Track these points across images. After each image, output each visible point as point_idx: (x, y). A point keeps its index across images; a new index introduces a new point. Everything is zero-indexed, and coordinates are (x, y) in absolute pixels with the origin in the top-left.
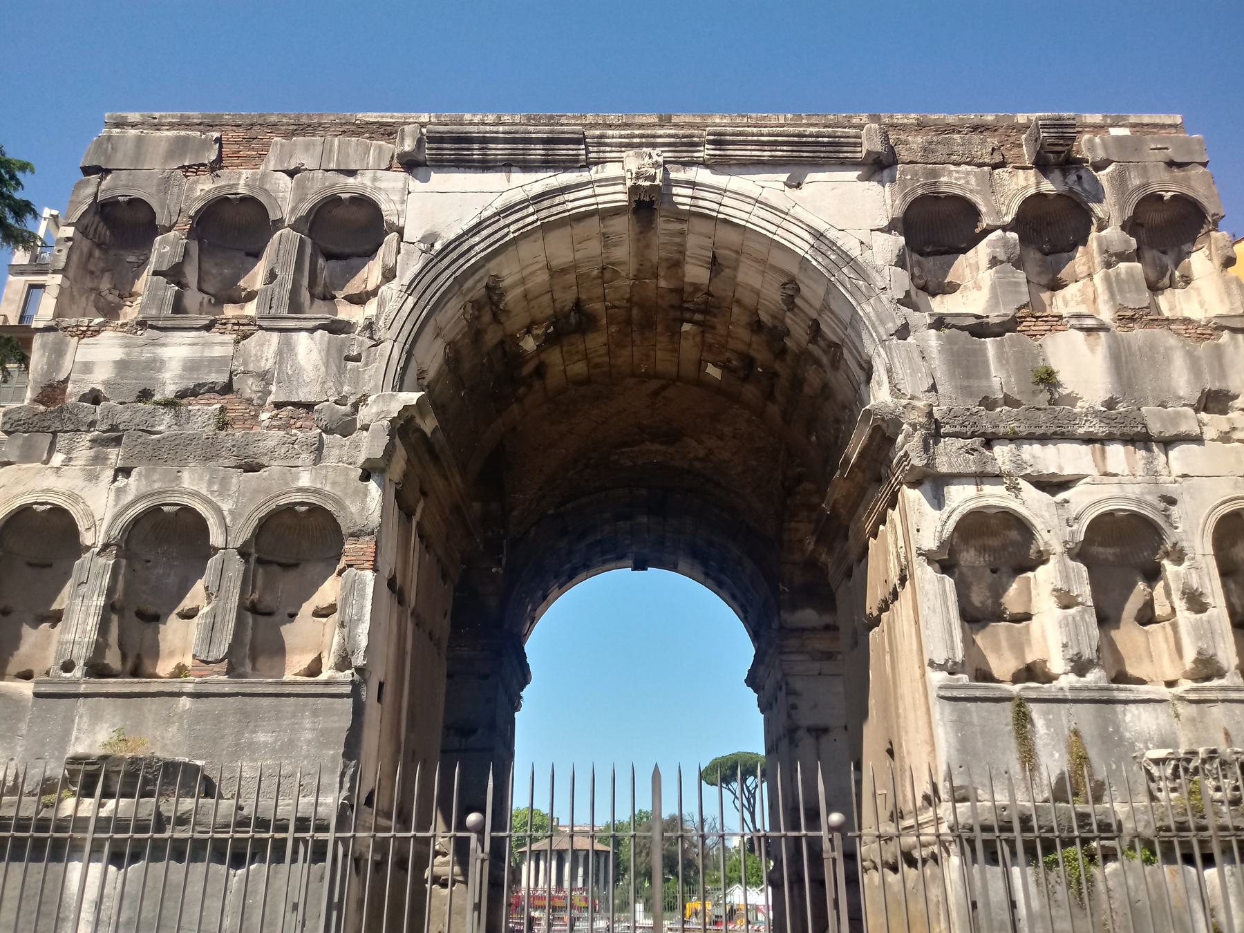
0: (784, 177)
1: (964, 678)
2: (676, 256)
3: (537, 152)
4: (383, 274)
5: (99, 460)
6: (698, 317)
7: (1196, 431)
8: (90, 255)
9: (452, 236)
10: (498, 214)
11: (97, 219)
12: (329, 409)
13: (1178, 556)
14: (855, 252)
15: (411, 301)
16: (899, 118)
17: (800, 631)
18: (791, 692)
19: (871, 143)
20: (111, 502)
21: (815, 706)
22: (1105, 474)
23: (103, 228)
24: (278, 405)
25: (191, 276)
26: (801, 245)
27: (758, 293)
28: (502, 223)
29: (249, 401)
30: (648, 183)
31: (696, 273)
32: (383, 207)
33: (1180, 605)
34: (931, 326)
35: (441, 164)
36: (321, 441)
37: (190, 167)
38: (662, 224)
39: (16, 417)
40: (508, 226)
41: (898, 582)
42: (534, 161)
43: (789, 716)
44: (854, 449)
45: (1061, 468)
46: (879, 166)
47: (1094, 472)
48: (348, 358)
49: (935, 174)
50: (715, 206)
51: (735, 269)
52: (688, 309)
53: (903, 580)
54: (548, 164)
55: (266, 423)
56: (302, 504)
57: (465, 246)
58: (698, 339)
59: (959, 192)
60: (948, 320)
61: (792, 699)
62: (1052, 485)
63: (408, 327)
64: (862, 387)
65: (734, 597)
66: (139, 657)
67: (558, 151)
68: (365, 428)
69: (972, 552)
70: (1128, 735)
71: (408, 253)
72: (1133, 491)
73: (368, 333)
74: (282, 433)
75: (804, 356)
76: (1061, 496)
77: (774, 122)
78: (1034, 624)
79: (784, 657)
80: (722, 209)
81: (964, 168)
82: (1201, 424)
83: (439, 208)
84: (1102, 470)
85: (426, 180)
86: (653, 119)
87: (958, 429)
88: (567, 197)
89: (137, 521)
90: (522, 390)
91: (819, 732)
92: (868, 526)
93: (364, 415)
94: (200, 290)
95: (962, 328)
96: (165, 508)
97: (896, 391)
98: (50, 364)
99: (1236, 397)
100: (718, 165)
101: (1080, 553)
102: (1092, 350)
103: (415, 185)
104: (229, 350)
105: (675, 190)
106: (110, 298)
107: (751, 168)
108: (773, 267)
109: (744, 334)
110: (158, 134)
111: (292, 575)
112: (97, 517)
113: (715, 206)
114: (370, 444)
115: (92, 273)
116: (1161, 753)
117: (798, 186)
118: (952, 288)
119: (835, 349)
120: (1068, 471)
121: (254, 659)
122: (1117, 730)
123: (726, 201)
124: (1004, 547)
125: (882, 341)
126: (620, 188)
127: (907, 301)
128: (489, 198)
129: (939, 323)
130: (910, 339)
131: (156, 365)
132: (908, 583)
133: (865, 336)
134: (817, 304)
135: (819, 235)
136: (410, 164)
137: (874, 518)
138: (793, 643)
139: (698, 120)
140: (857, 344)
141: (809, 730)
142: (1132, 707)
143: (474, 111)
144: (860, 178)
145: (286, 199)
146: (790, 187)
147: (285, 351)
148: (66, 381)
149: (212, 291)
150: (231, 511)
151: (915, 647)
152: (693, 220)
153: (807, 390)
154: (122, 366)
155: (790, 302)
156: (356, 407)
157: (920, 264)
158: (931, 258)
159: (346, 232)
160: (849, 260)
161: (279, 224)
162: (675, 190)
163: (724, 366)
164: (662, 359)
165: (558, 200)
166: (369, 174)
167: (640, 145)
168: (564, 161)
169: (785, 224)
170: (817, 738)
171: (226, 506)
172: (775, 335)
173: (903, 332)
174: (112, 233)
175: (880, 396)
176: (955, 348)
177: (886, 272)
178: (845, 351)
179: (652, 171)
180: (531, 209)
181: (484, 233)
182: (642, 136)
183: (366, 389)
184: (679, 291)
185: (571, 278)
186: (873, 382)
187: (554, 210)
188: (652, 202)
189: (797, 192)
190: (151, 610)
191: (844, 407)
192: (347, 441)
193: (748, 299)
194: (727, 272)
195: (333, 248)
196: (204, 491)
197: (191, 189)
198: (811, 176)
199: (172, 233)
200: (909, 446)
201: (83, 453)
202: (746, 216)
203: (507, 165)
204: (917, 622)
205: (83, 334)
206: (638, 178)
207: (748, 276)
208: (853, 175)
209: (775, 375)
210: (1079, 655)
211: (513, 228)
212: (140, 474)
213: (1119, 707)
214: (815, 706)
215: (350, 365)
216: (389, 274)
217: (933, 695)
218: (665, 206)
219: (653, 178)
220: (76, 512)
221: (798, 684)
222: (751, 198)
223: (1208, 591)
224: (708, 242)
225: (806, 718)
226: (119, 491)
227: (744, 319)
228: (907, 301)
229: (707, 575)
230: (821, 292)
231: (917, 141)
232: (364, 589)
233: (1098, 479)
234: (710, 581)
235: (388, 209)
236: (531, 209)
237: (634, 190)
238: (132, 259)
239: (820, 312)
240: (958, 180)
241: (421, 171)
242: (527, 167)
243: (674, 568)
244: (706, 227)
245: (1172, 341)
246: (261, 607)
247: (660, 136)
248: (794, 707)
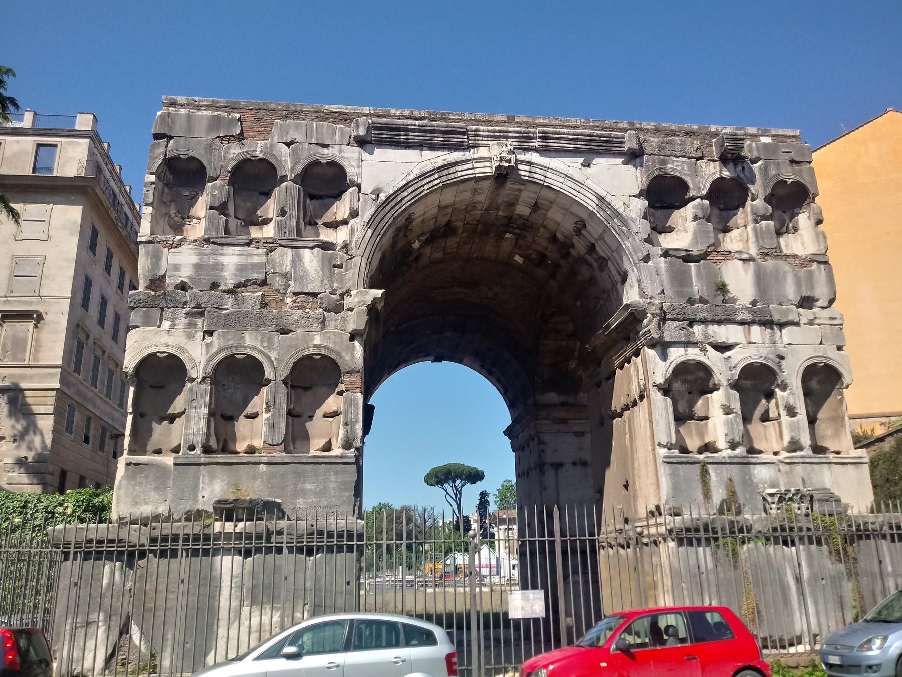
0: (581, 160)
1: (676, 452)
2: (513, 200)
3: (439, 139)
4: (350, 213)
5: (192, 325)
6: (517, 231)
7: (796, 320)
8: (163, 192)
9: (392, 192)
10: (417, 178)
11: (166, 168)
13: (784, 387)
14: (621, 210)
15: (370, 232)
16: (645, 125)
17: (548, 406)
18: (541, 442)
19: (630, 144)
20: (204, 352)
21: (555, 451)
23: (168, 173)
24: (296, 294)
25: (231, 210)
27: (559, 224)
28: (420, 184)
29: (278, 291)
30: (507, 165)
31: (522, 209)
32: (347, 170)
33: (783, 413)
34: (662, 256)
35: (382, 143)
37: (224, 137)
38: (509, 184)
39: (137, 298)
40: (423, 185)
41: (637, 398)
42: (437, 144)
43: (540, 457)
44: (615, 322)
45: (727, 339)
46: (634, 157)
47: (744, 341)
48: (335, 266)
49: (664, 163)
50: (543, 178)
51: (547, 210)
52: (512, 227)
53: (642, 397)
54: (445, 147)
55: (290, 305)
56: (317, 354)
57: (399, 198)
58: (513, 242)
59: (678, 174)
60: (671, 252)
61: (541, 447)
62: (722, 347)
63: (369, 248)
64: (619, 285)
65: (499, 381)
66: (225, 441)
67: (451, 139)
68: (351, 310)
69: (679, 382)
70: (755, 481)
71: (365, 200)
72: (764, 351)
73: (345, 250)
75: (581, 260)
76: (727, 354)
77: (574, 124)
78: (710, 422)
79: (538, 422)
80: (546, 179)
81: (681, 159)
82: (799, 315)
83: (383, 171)
85: (372, 153)
86: (504, 118)
87: (675, 316)
88: (460, 168)
89: (220, 363)
90: (405, 268)
91: (558, 466)
92: (617, 363)
93: (348, 302)
94: (235, 217)
95: (678, 257)
97: (643, 294)
98: (152, 264)
99: (818, 300)
100: (543, 151)
101: (735, 385)
102: (746, 272)
103: (365, 156)
104: (263, 259)
105: (520, 167)
106: (176, 219)
107: (562, 154)
108: (572, 213)
109: (544, 243)
110: (200, 113)
111: (309, 394)
112: (197, 361)
113: (543, 178)
115: (165, 203)
116: (773, 491)
117: (589, 166)
118: (671, 230)
119: (603, 262)
120: (731, 341)
121: (294, 442)
122: (750, 479)
123: (549, 174)
124: (695, 380)
125: (636, 264)
126: (488, 164)
127: (649, 240)
128: (411, 167)
129: (666, 253)
130: (650, 263)
132: (645, 399)
133: (625, 258)
134: (596, 236)
135: (601, 199)
136: (362, 143)
137: (622, 359)
138: (544, 413)
139: (530, 120)
140: (619, 262)
141: (552, 465)
142: (758, 466)
143: (397, 108)
144: (623, 163)
145: (287, 162)
146: (584, 166)
147: (297, 261)
148: (164, 276)
149: (241, 217)
150: (275, 358)
151: (649, 433)
152: (528, 184)
153: (579, 277)
154: (198, 267)
155: (578, 232)
156: (342, 296)
157: (653, 214)
158: (659, 211)
160: (618, 215)
161: (284, 178)
162: (520, 167)
163: (527, 258)
164: (489, 250)
165: (452, 170)
166: (337, 147)
167: (499, 137)
168: (455, 145)
169: (582, 190)
170: (556, 470)
171: (273, 355)
172: (565, 248)
173: (647, 259)
174: (174, 177)
175: (631, 296)
176: (675, 269)
178: (610, 263)
179: (509, 157)
180: (437, 176)
181: (410, 190)
182: (500, 132)
183: (348, 286)
184: (510, 218)
185: (450, 210)
186: (626, 284)
187: (450, 177)
188: (507, 174)
189: (588, 170)
190: (229, 413)
191: (604, 292)
193: (551, 226)
194: (542, 211)
195: (313, 192)
196: (259, 346)
197: (227, 153)
198: (597, 161)
199: (218, 182)
200: (650, 325)
201: (182, 321)
202: (560, 185)
203: (420, 146)
204: (651, 421)
206: (501, 161)
207: (555, 214)
208: (620, 161)
209: (557, 266)
211: (426, 187)
212: (219, 335)
213: (752, 466)
214: (555, 451)
215: (337, 270)
216: (354, 214)
217: (660, 461)
218: (514, 176)
219: (509, 161)
220: (184, 357)
221: (546, 438)
222: (562, 172)
223: (798, 406)
224: (535, 196)
225: (550, 457)
226: (209, 346)
227: (546, 235)
228: (649, 240)
229: (482, 366)
230: (600, 231)
231: (655, 141)
232: (357, 404)
234: (484, 371)
235: (351, 171)
236: (437, 176)
237: (499, 168)
238: (186, 193)
239: (597, 240)
240: (677, 167)
241: (368, 147)
242: (433, 148)
243: (460, 361)
244: (536, 188)
245: (787, 268)
246: (294, 412)
247: (511, 132)
248: (543, 451)
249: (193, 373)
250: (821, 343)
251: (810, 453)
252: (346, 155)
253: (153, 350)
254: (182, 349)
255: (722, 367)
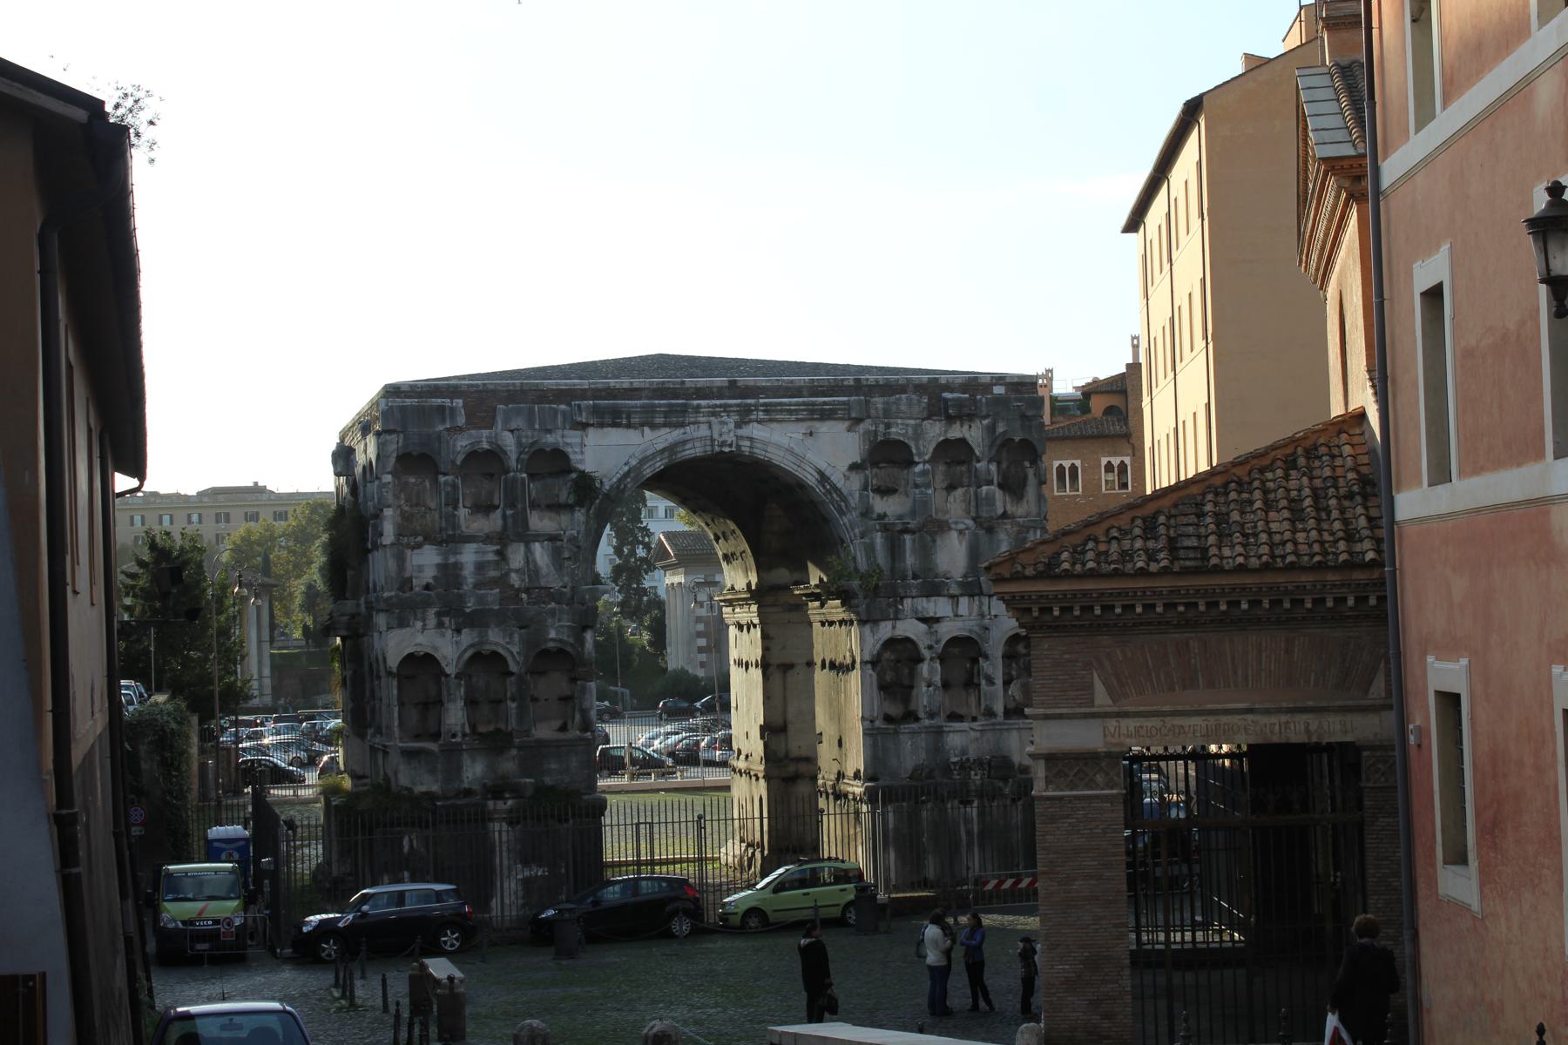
5: (440, 625)
13: (986, 657)
26: (811, 479)
33: (983, 682)
101: (942, 658)
131: (458, 566)
135: (821, 473)
166: (560, 432)
177: (857, 495)
201: (432, 621)
205: (413, 548)
240: (899, 430)
249: (448, 670)
252: (568, 440)
254: (436, 649)
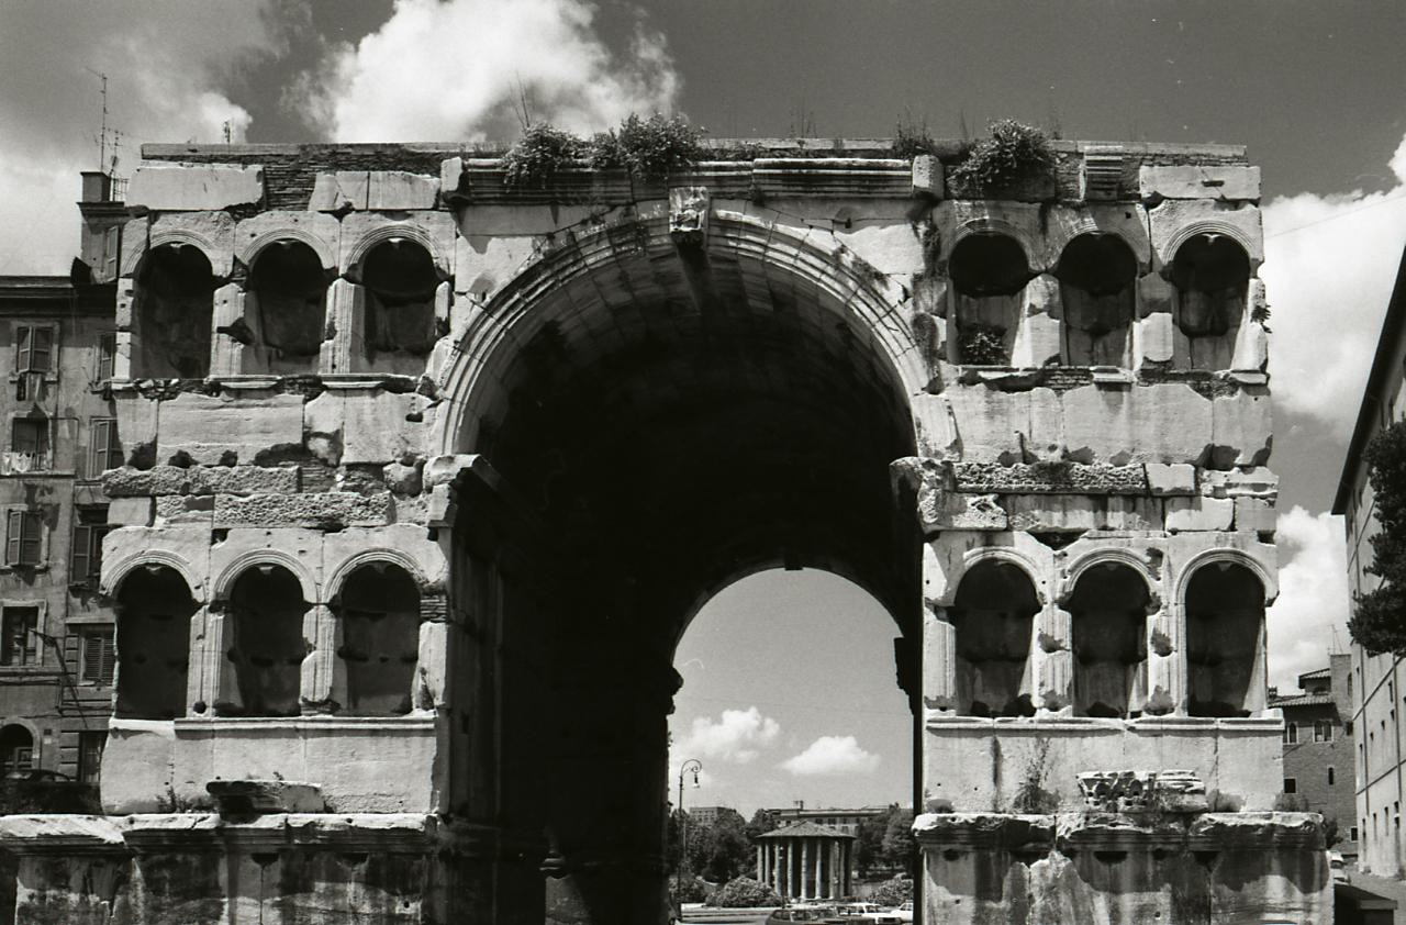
7: (1189, 484)
12: (398, 473)
22: (1105, 528)
24: (351, 467)
29: (324, 462)
36: (393, 504)
55: (340, 485)
74: (356, 494)
84: (1101, 525)
96: (262, 568)
99: (1236, 454)
114: (436, 505)
116: (1090, 775)
145: (337, 247)
159: (399, 282)
161: (332, 274)
192: (415, 502)
202: (791, 261)
210: (1053, 692)
223: (1173, 637)
233: (1095, 532)
250: (1232, 528)
251: (1185, 716)
253: (140, 561)
255: (1050, 574)
